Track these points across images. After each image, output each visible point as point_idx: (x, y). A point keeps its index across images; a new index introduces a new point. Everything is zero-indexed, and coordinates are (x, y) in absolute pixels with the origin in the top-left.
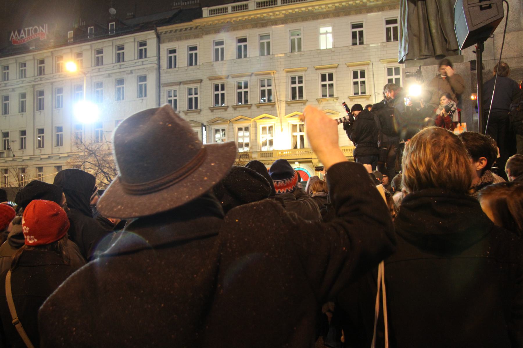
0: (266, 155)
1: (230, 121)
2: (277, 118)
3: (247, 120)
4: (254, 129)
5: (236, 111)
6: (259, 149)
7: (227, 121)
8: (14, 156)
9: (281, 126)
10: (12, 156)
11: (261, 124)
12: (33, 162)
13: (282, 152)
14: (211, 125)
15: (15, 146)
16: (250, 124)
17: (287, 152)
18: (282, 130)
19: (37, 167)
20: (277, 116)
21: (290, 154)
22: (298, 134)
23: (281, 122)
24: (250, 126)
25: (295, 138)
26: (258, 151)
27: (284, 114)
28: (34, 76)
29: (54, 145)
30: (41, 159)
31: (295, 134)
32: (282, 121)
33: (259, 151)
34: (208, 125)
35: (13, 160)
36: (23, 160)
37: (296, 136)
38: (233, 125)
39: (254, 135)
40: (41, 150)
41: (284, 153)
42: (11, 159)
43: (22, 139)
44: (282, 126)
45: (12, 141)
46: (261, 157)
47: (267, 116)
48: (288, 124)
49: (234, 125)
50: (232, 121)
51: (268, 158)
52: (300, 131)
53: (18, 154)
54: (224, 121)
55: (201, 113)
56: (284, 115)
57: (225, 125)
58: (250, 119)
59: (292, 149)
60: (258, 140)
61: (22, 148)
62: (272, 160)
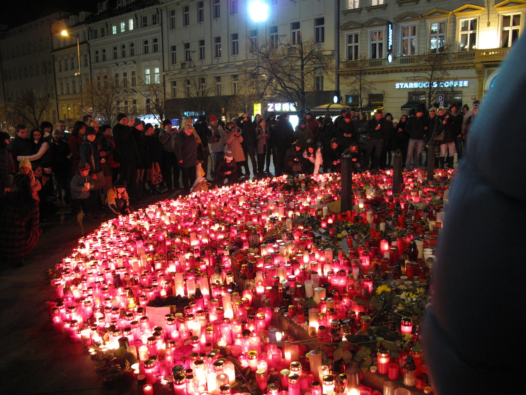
1: (422, 16)
2: (483, 8)
3: (443, 13)
4: (452, 24)
6: (456, 50)
7: (419, 17)
8: (195, 66)
9: (488, 19)
10: (193, 66)
11: (461, 18)
12: (212, 72)
13: (487, 51)
14: (398, 22)
15: (195, 57)
16: (448, 19)
17: (495, 52)
18: (489, 24)
19: (215, 77)
20: (484, 7)
21: (497, 54)
22: (510, 29)
23: (489, 14)
24: (447, 22)
25: (505, 34)
26: (455, 52)
27: (494, 4)
29: (230, 54)
30: (219, 68)
31: (506, 29)
32: (490, 12)
33: (458, 52)
34: (395, 22)
35: (194, 70)
36: (203, 70)
37: (508, 31)
38: (425, 21)
39: (451, 32)
40: (218, 59)
41: (490, 53)
42: (191, 70)
44: (489, 20)
45: (193, 52)
47: (470, 7)
48: (499, 15)
49: (427, 21)
50: (425, 16)
52: (514, 25)
53: (198, 63)
54: (414, 16)
55: (388, 8)
56: (494, 4)
57: (415, 22)
58: (448, 12)
59: (500, 48)
60: (456, 39)
61: (201, 58)
62: (473, 63)
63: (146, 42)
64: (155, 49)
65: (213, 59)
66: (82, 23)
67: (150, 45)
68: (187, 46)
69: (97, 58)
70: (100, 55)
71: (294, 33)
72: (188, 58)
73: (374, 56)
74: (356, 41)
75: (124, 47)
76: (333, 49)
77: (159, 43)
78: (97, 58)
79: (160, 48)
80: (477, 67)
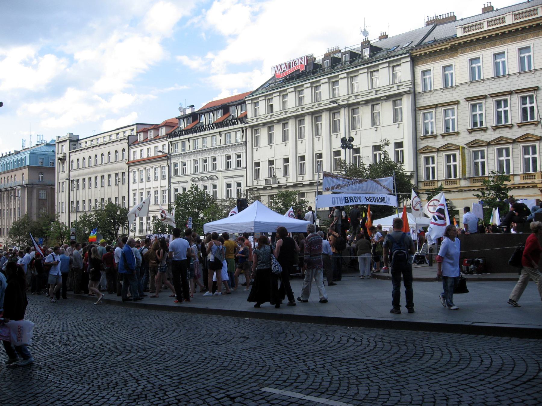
0: (529, 178)
5: (496, 132)
8: (279, 182)
28: (296, 107)
33: (522, 173)
43: (285, 166)
46: (524, 179)
51: (531, 180)
63: (229, 157)
64: (238, 164)
65: (298, 176)
66: (163, 137)
67: (233, 160)
68: (271, 162)
69: (176, 171)
70: (179, 168)
71: (376, 155)
72: (272, 175)
73: (449, 175)
74: (433, 163)
75: (205, 161)
76: (412, 170)
77: (243, 159)
78: (176, 171)
79: (243, 165)
80: (538, 186)
